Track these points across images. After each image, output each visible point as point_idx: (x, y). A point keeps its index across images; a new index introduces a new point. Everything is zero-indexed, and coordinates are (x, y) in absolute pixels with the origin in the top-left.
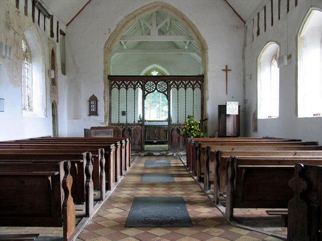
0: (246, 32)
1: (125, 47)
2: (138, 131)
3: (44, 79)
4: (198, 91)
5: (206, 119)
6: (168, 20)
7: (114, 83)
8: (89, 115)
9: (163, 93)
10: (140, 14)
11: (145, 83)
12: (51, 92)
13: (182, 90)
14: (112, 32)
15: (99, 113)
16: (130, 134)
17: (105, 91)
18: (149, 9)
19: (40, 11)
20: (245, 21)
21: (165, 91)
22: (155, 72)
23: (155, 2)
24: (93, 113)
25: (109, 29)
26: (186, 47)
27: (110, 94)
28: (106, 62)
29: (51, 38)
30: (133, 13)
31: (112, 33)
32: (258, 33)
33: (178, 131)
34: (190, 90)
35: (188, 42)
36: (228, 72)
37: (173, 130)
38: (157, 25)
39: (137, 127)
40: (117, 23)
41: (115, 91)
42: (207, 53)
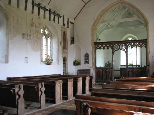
2: (110, 72)
3: (58, 47)
4: (144, 48)
5: (149, 65)
7: (97, 46)
8: (85, 63)
10: (110, 8)
11: (113, 45)
12: (62, 53)
14: (95, 19)
15: (89, 63)
16: (106, 73)
17: (92, 51)
21: (125, 49)
22: (130, 38)
23: (117, 1)
24: (87, 62)
25: (94, 19)
27: (95, 52)
29: (63, 27)
30: (105, 8)
31: (95, 20)
33: (132, 72)
37: (129, 71)
39: (110, 69)
40: (97, 15)
41: (98, 50)
42: (148, 26)
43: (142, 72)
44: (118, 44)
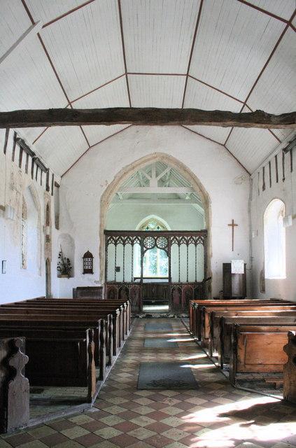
0: (251, 185)
1: (121, 198)
4: (200, 246)
6: (167, 170)
7: (110, 239)
8: (84, 273)
9: (164, 249)
10: (140, 164)
13: (183, 246)
16: (127, 294)
17: (100, 248)
18: (149, 160)
19: (38, 166)
20: (251, 172)
24: (88, 271)
25: (106, 181)
26: (187, 198)
27: (106, 250)
28: (102, 216)
32: (264, 188)
33: (179, 290)
34: (192, 246)
35: (189, 193)
36: (235, 227)
38: (157, 176)
41: (111, 246)
43: (197, 290)
44: (153, 237)
